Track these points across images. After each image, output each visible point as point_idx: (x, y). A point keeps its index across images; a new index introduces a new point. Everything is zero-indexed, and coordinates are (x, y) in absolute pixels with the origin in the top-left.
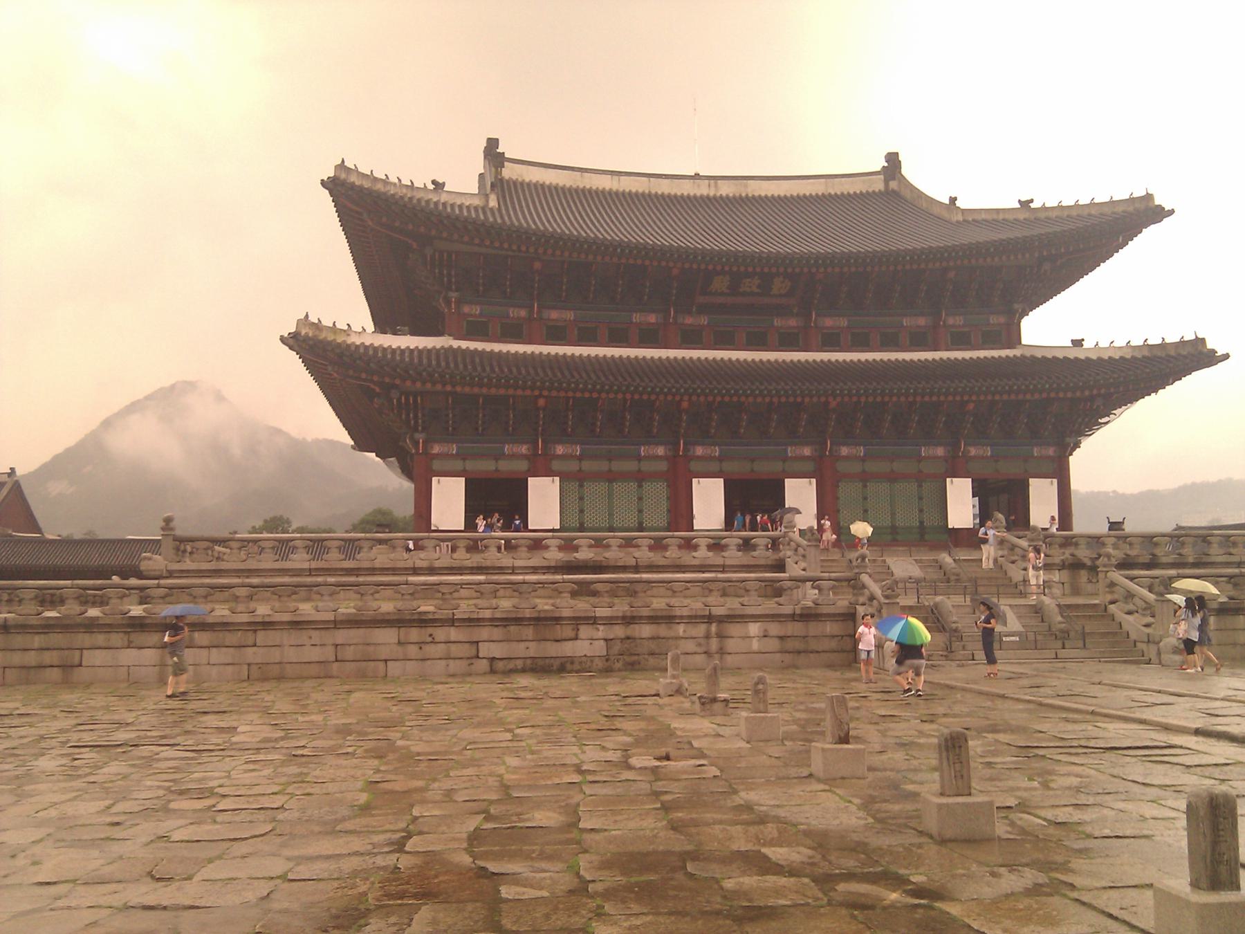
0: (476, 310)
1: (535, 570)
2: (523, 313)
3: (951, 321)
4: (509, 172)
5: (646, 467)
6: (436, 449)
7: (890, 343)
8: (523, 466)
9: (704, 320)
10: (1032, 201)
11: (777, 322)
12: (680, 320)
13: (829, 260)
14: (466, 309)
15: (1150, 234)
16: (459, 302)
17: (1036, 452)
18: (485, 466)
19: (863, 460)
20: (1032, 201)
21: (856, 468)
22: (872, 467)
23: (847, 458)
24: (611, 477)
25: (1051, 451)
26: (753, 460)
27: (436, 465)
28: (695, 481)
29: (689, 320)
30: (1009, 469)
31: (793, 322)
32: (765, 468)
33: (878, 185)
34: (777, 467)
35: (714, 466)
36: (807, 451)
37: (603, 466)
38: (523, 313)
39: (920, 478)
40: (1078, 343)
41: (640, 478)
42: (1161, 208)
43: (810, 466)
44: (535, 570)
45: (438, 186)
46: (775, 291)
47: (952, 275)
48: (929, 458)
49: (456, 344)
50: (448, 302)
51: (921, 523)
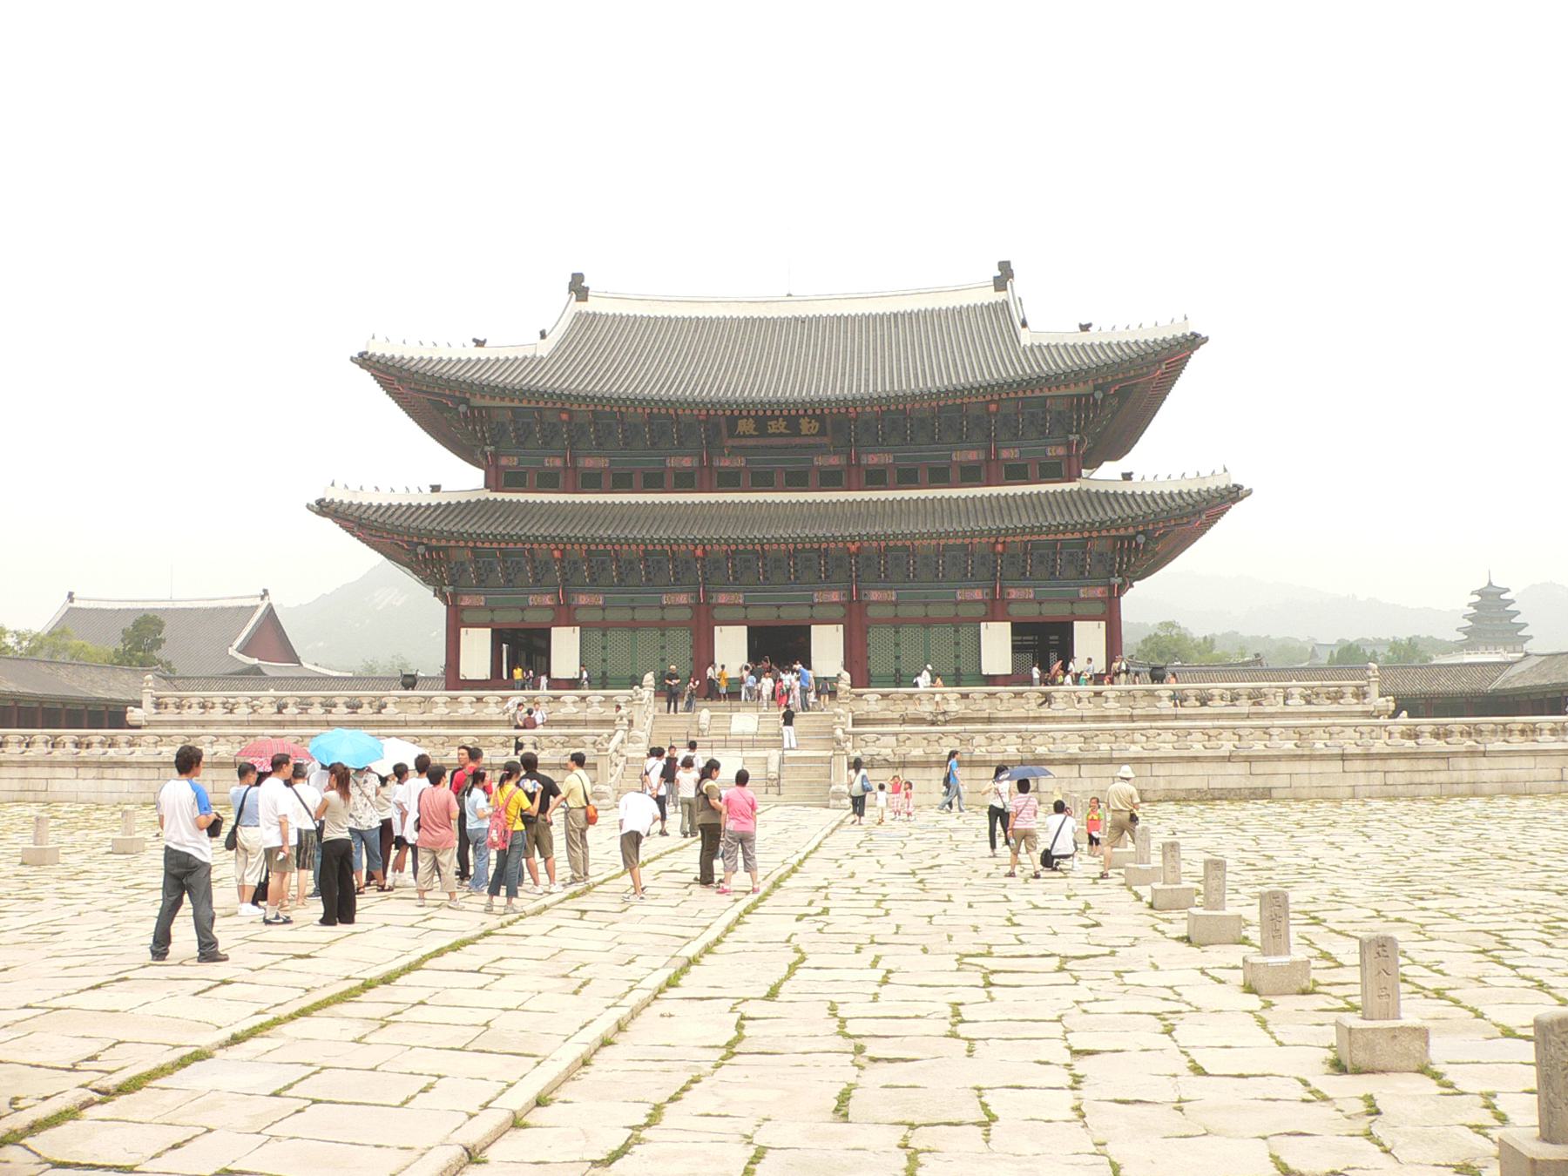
0: (514, 461)
1: (424, 723)
2: (558, 462)
3: (1004, 454)
4: (591, 306)
5: (670, 615)
6: (466, 601)
7: (940, 477)
8: (547, 616)
9: (740, 462)
10: (1090, 325)
11: (819, 461)
12: (716, 464)
13: (844, 403)
14: (504, 461)
15: (1197, 358)
16: (496, 456)
17: (1083, 593)
18: (510, 618)
19: (896, 604)
20: (1090, 325)
21: (889, 612)
22: (904, 611)
23: (877, 603)
24: (634, 626)
25: (1098, 592)
26: (779, 607)
27: (466, 616)
28: (717, 628)
29: (724, 463)
30: (1054, 611)
31: (835, 461)
32: (791, 615)
33: (991, 296)
34: (805, 613)
35: (740, 613)
36: (835, 596)
37: (625, 615)
38: (558, 462)
39: (956, 622)
40: (1127, 477)
41: (663, 626)
42: (1196, 336)
43: (840, 612)
44: (424, 723)
45: (480, 343)
46: (804, 430)
47: (993, 407)
48: (966, 601)
49: (492, 496)
50: (484, 454)
51: (957, 669)
